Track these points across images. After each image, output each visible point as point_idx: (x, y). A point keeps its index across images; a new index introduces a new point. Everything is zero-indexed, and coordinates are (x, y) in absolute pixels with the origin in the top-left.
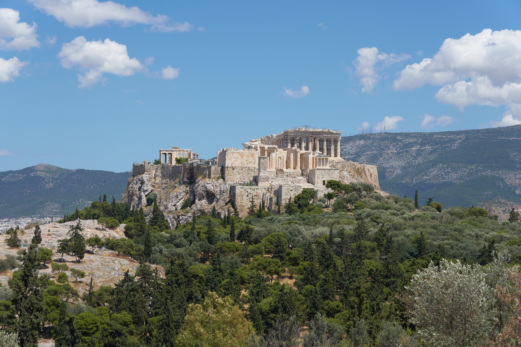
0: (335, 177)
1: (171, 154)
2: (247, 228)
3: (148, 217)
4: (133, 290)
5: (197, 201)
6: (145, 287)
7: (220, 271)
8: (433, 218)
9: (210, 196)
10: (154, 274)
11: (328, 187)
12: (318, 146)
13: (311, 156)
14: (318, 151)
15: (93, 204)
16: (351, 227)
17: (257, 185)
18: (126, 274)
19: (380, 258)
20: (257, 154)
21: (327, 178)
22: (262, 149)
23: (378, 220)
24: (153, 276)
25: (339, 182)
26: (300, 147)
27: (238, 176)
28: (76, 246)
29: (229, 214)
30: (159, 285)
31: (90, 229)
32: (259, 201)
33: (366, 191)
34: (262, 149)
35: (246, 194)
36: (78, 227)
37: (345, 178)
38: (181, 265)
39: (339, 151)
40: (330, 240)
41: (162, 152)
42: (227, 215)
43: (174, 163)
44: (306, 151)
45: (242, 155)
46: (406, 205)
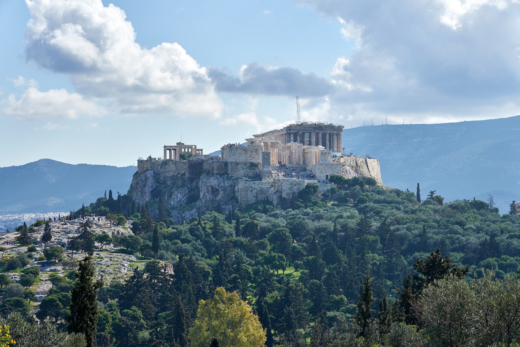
5: (201, 196)
8: (436, 211)
9: (215, 191)
12: (321, 140)
16: (354, 220)
23: (381, 214)
27: (242, 172)
32: (263, 196)
33: (369, 185)
35: (250, 189)
38: (186, 261)
40: (333, 234)
41: (166, 148)
42: (231, 209)
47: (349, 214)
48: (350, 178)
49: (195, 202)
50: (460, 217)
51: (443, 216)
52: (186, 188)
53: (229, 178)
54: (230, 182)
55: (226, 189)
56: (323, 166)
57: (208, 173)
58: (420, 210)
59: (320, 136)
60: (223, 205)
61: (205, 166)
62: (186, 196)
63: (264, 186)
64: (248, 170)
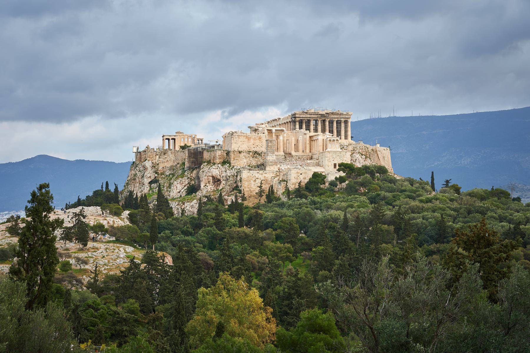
0: (347, 160)
1: (174, 139)
2: (256, 212)
3: (152, 205)
4: (139, 276)
6: (152, 274)
7: (229, 256)
8: (452, 200)
9: (216, 181)
10: (161, 261)
11: (339, 170)
14: (327, 133)
17: (265, 170)
18: (132, 261)
19: (397, 243)
20: (265, 137)
21: (338, 161)
22: (270, 131)
23: (394, 203)
24: (160, 263)
26: (308, 129)
27: (245, 160)
28: (81, 233)
29: (236, 200)
30: (166, 272)
31: (93, 215)
34: (270, 131)
36: (81, 214)
37: (357, 161)
38: (188, 252)
39: (349, 133)
40: (345, 225)
41: (165, 138)
42: (234, 201)
43: (177, 148)
44: (316, 134)
45: (248, 138)
46: (423, 188)
47: (359, 203)
48: (359, 166)
49: (195, 192)
50: (479, 204)
51: (461, 204)
52: (186, 178)
53: (231, 167)
54: (234, 172)
55: (227, 179)
56: (331, 154)
57: (209, 162)
59: (327, 123)
60: (225, 195)
61: (206, 156)
62: (186, 188)
63: (269, 176)
64: (251, 159)
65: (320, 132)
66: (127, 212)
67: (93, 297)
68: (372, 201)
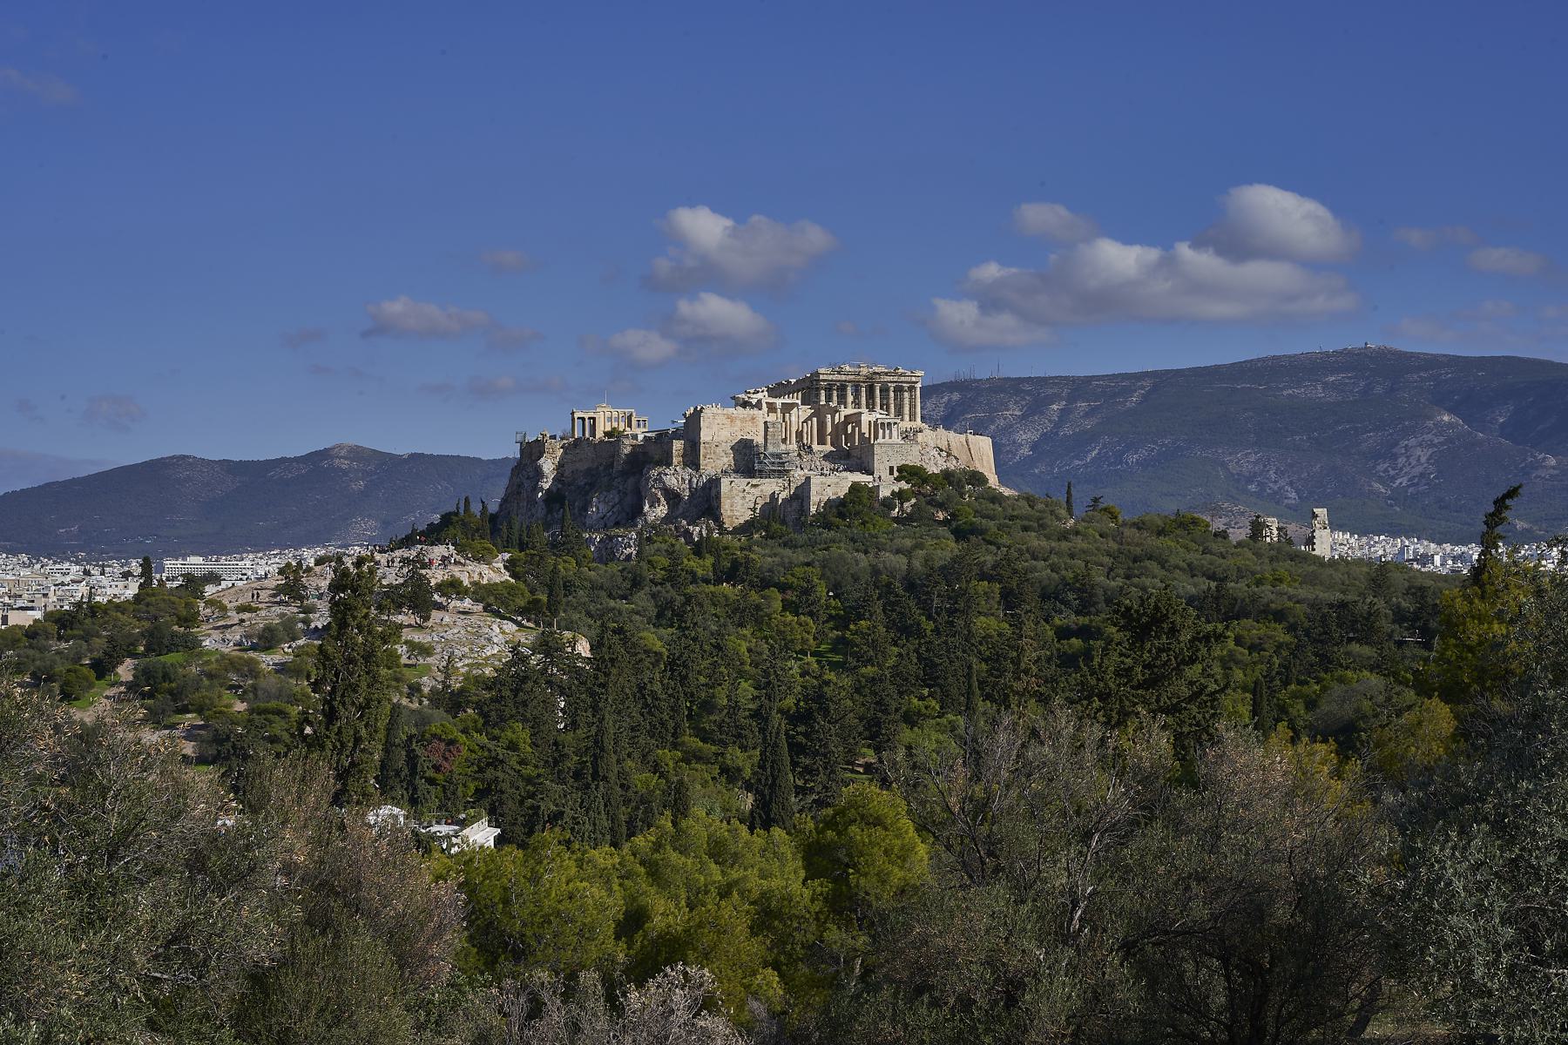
0: (913, 459)
4: (524, 679)
5: (646, 508)
9: (672, 497)
12: (878, 400)
13: (867, 418)
15: (443, 517)
18: (514, 650)
25: (921, 469)
26: (842, 400)
27: (725, 460)
30: (579, 671)
38: (619, 631)
45: (731, 419)
58: (1077, 533)
65: (864, 410)
66: (507, 556)
67: (441, 721)
68: (959, 534)
